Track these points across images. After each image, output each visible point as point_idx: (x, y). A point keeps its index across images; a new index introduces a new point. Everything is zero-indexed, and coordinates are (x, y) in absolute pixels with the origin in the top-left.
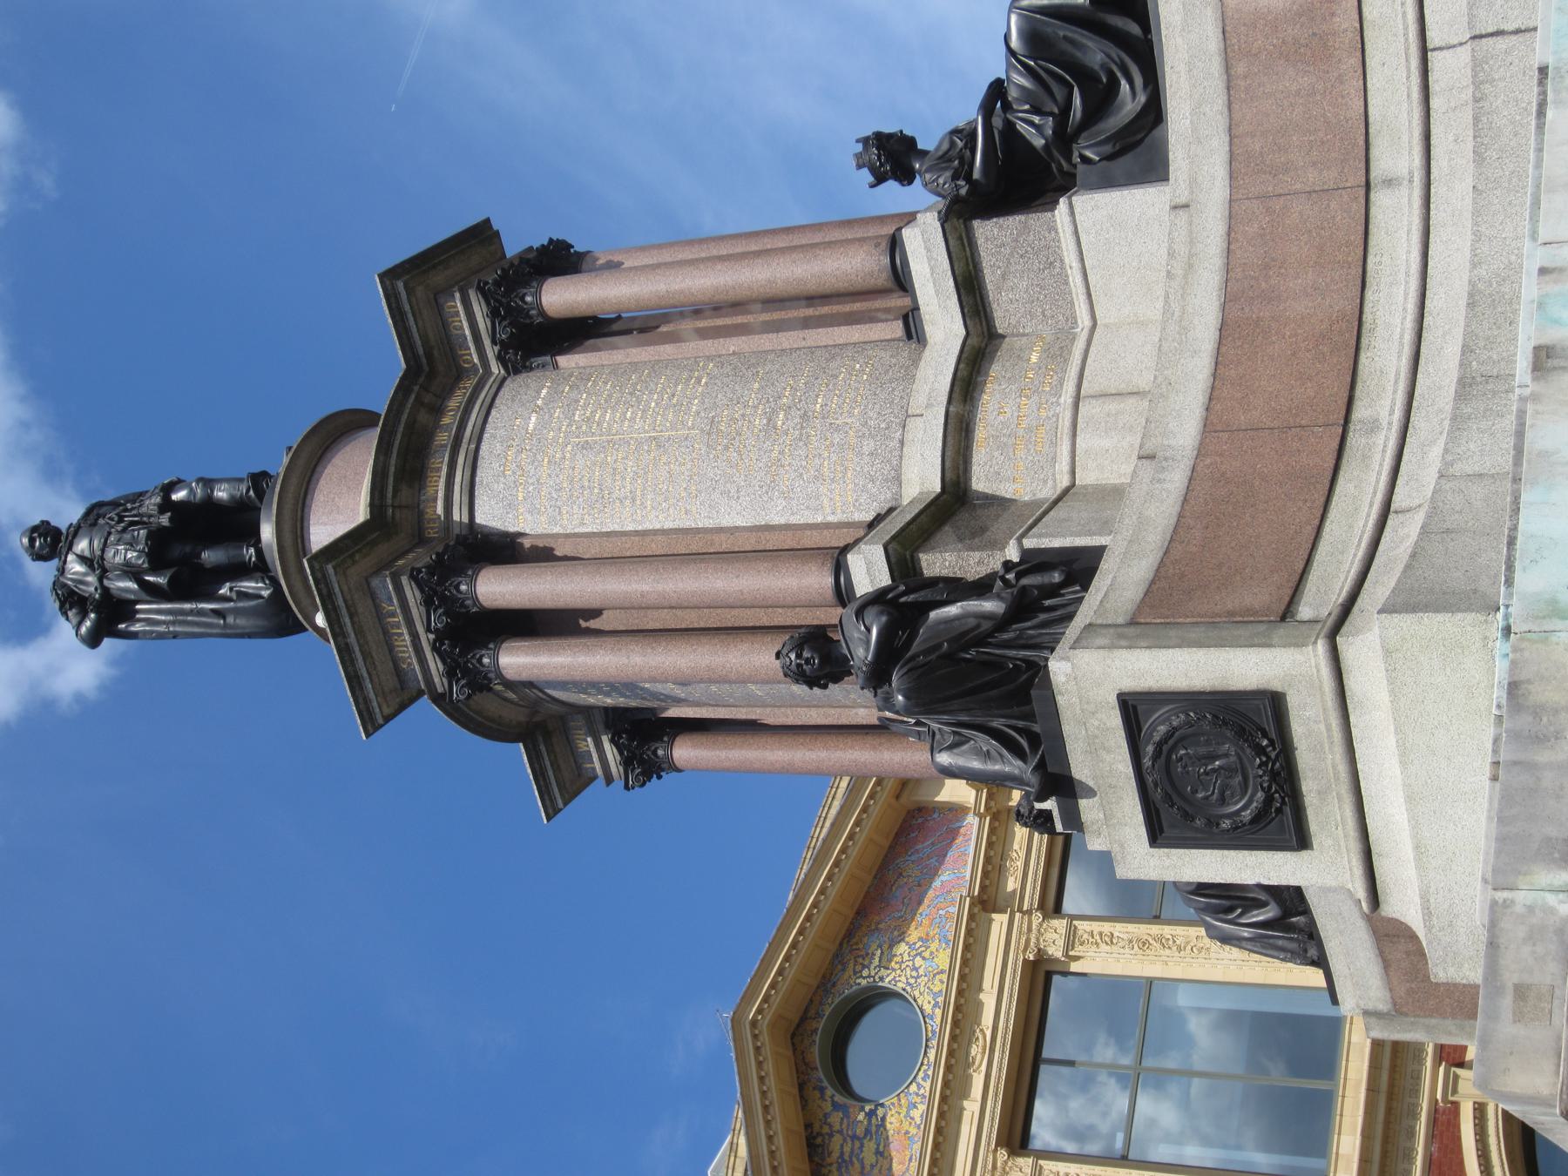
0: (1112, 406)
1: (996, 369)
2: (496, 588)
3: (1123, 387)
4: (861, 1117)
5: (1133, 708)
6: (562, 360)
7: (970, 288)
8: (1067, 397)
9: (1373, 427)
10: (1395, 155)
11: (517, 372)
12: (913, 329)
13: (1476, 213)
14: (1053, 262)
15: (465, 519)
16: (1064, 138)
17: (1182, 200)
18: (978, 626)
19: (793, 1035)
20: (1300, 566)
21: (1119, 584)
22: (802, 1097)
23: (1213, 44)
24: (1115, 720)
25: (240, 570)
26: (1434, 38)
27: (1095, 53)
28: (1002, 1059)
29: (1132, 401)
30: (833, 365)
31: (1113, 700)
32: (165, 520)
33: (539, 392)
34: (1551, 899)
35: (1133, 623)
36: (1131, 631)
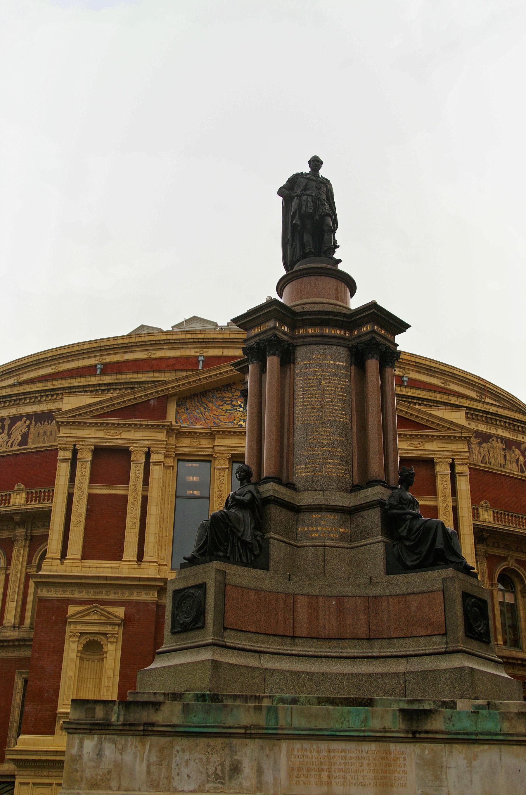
2: (272, 362)
4: (239, 403)
6: (353, 367)
12: (355, 488)
16: (401, 539)
18: (240, 531)
24: (200, 582)
27: (424, 549)
31: (205, 581)
32: (317, 217)
33: (342, 362)
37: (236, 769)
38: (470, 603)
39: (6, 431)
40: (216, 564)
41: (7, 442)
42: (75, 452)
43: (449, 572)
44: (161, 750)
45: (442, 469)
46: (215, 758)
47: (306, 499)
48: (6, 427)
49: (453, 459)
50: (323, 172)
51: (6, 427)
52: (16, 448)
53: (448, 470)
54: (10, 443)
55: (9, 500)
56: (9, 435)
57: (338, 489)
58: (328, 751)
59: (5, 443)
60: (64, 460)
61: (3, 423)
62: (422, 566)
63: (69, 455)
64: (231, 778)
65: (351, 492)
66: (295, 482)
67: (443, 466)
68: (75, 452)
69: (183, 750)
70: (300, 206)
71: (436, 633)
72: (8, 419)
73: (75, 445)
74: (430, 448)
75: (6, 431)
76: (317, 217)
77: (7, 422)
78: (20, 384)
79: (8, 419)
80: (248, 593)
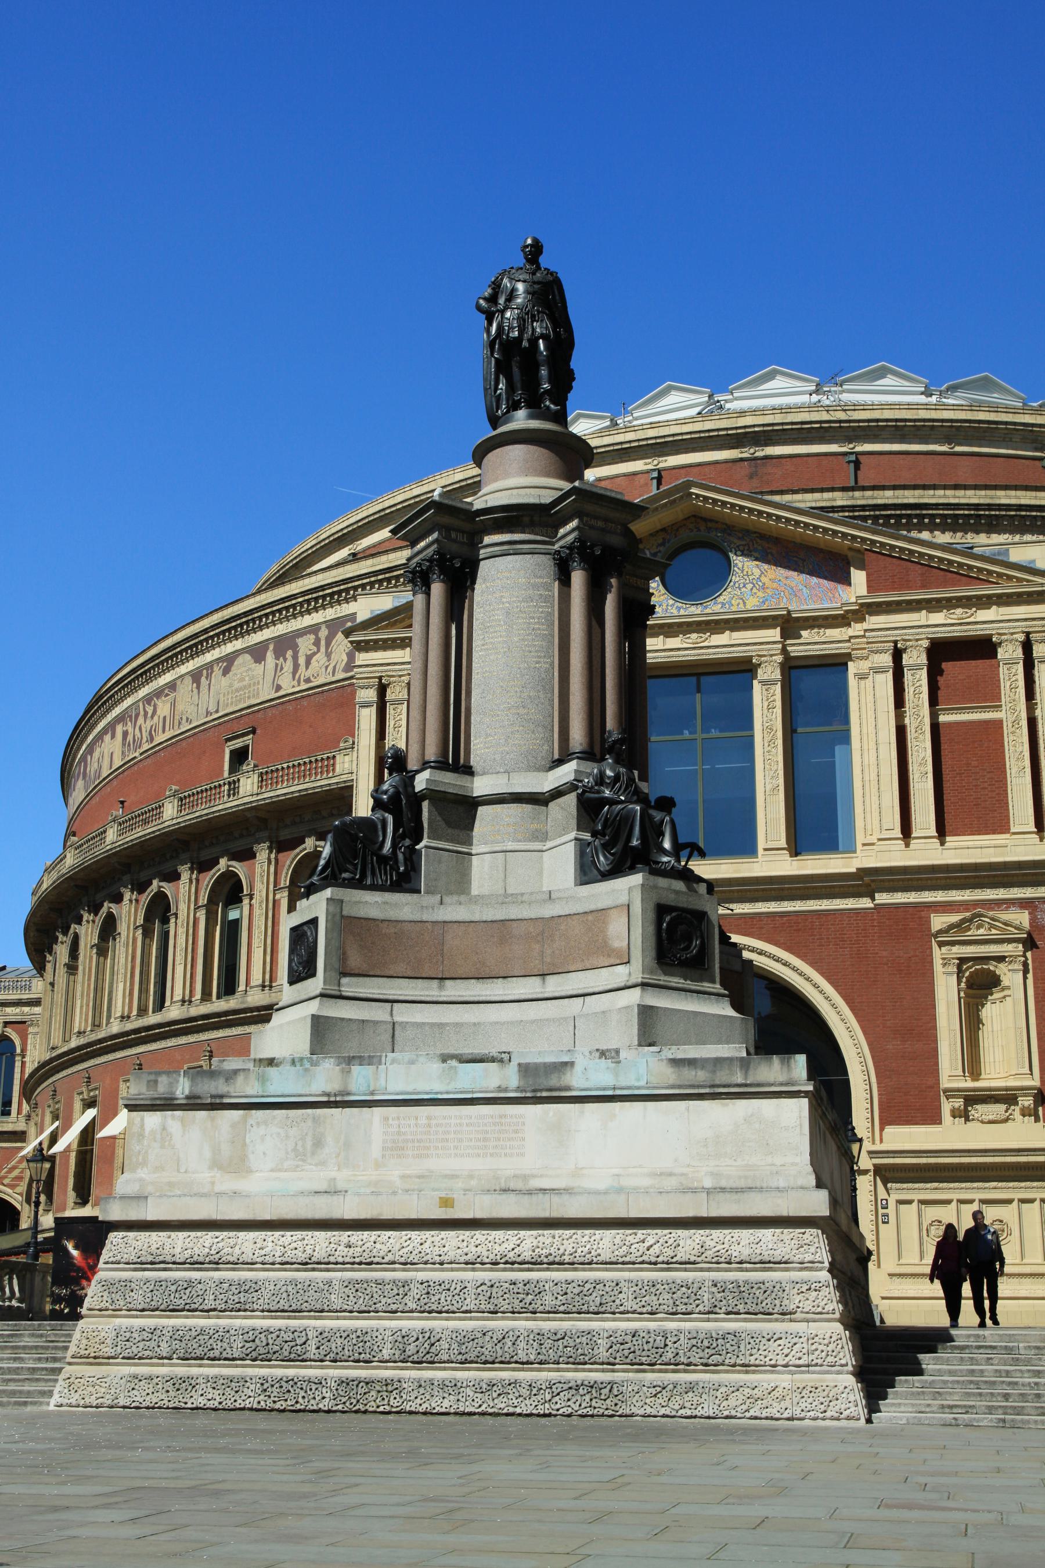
0: (501, 868)
1: (530, 806)
2: (437, 589)
3: (508, 871)
5: (314, 922)
7: (557, 793)
8: (510, 846)
9: (441, 988)
10: (554, 985)
11: (554, 559)
13: (512, 1023)
14: (565, 831)
15: (481, 557)
17: (553, 896)
19: (694, 516)
20: (371, 973)
21: (371, 904)
22: (657, 532)
23: (600, 905)
25: (511, 387)
26: (587, 998)
28: (691, 656)
29: (503, 876)
30: (540, 729)
33: (540, 577)
34: (180, 1088)
35: (342, 916)
36: (338, 917)
37: (318, 1143)
38: (668, 919)
39: (323, 649)
40: (328, 892)
41: (327, 667)
42: (382, 690)
43: (636, 879)
44: (234, 1126)
45: (1010, 652)
46: (292, 1132)
47: (481, 786)
48: (323, 643)
49: (1028, 634)
50: (544, 261)
51: (323, 643)
52: (341, 675)
53: (1019, 653)
54: (330, 669)
55: (334, 765)
56: (328, 655)
57: (529, 769)
58: (429, 1118)
59: (324, 669)
60: (366, 705)
61: (317, 635)
62: (615, 871)
63: (371, 695)
64: (313, 1154)
65: (551, 768)
66: (472, 763)
67: (1010, 648)
68: (382, 690)
69: (258, 1124)
70: (500, 328)
71: (618, 962)
72: (323, 627)
73: (380, 678)
74: (986, 619)
75: (323, 649)
76: (525, 344)
77: (324, 633)
78: (355, 557)
79: (323, 627)
80: (378, 925)
